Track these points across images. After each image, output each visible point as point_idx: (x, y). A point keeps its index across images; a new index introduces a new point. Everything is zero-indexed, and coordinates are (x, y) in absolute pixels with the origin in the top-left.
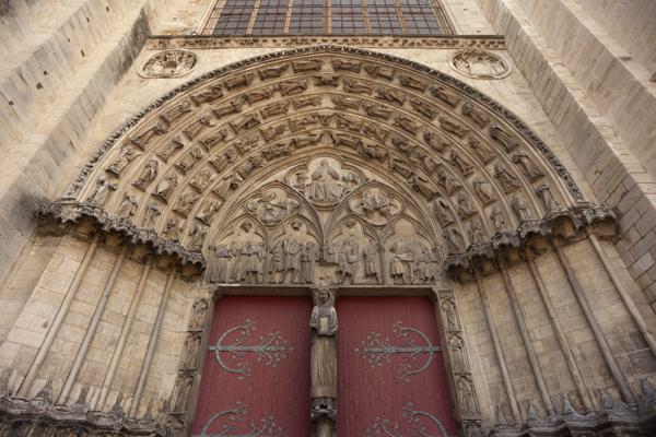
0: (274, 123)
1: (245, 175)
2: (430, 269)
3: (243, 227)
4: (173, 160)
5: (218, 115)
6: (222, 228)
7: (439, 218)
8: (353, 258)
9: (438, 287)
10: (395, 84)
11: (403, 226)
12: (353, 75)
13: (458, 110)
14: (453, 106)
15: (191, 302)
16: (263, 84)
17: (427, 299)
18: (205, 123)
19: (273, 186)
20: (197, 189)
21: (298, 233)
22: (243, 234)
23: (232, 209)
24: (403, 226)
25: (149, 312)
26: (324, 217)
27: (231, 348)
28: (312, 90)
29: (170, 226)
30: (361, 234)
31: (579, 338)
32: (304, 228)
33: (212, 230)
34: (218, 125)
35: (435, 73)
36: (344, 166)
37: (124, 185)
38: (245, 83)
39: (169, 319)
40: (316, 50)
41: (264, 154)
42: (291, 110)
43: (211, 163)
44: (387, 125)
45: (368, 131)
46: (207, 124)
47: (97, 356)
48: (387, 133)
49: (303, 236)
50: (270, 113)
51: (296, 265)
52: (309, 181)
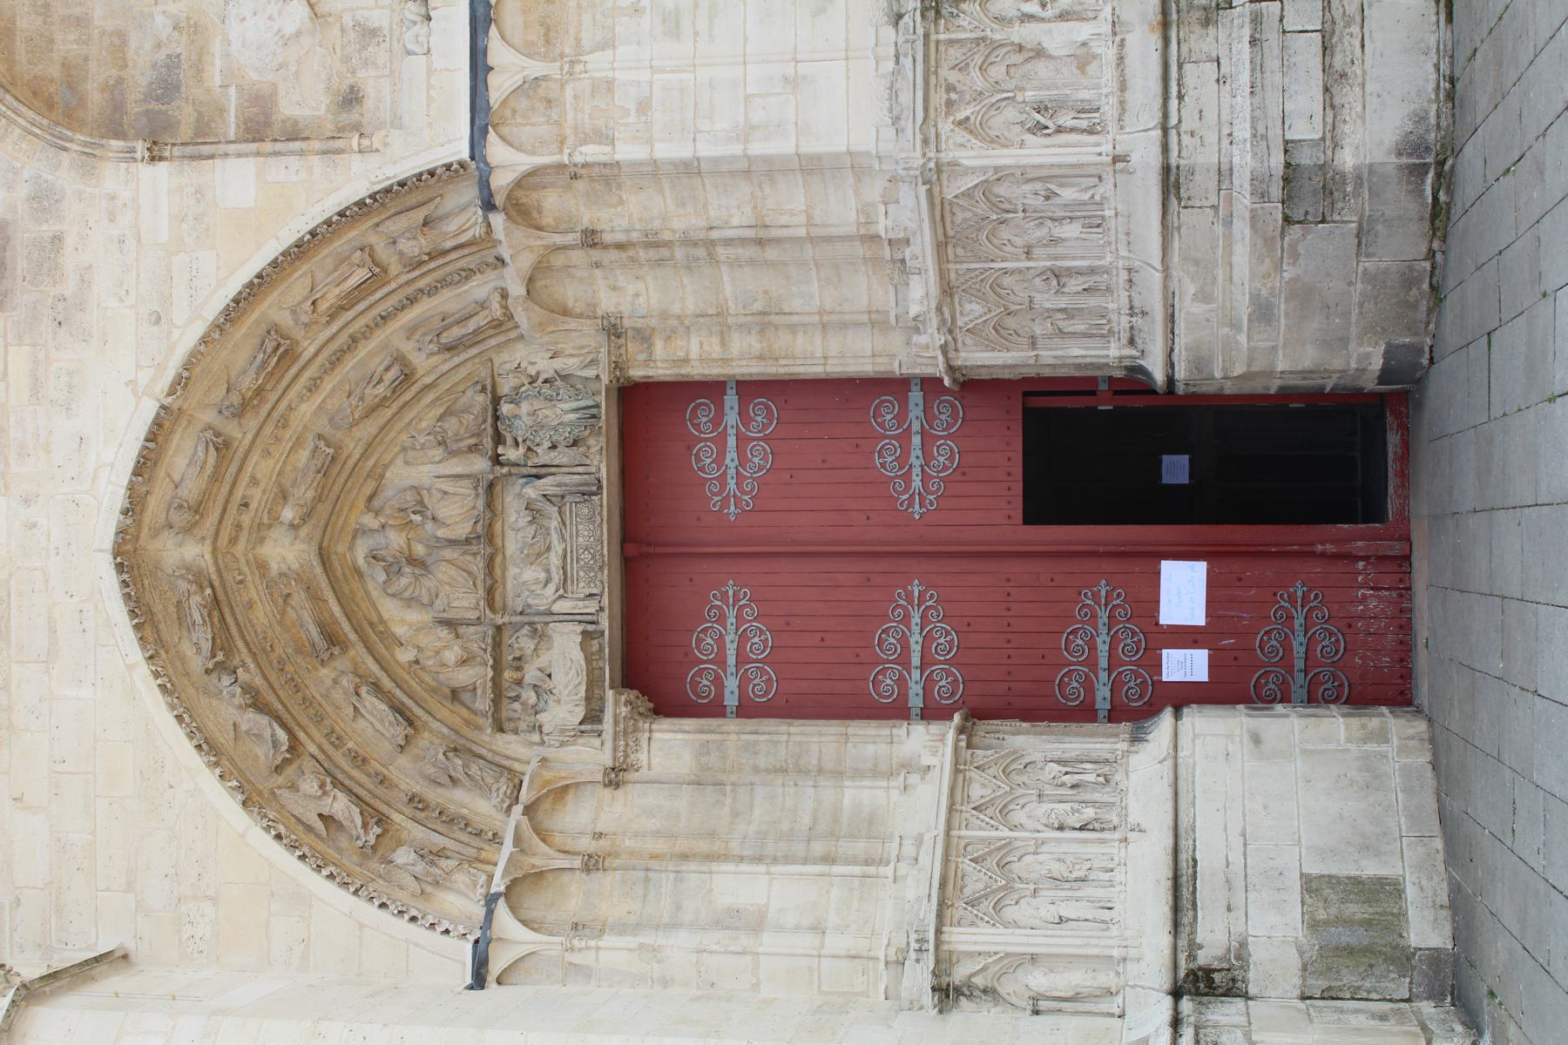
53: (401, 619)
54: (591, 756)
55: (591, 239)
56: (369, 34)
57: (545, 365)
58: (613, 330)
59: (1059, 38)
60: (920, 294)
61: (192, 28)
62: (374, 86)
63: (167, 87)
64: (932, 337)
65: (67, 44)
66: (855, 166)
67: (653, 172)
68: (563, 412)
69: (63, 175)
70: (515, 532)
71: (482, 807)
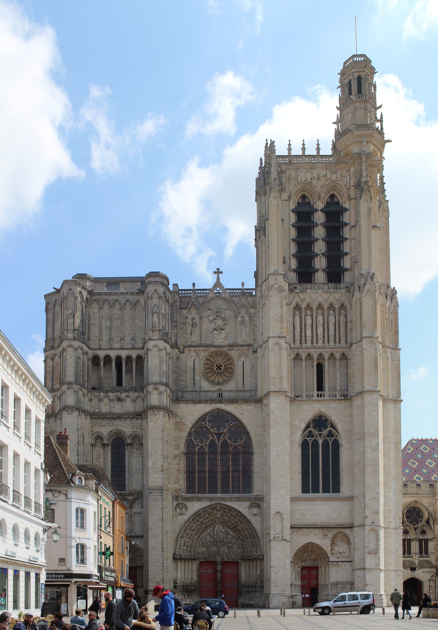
0: (206, 521)
1: (201, 534)
2: (238, 557)
3: (202, 547)
4: (188, 537)
5: (194, 523)
6: (198, 547)
7: (242, 547)
8: (225, 554)
9: (239, 561)
10: (234, 514)
11: (235, 546)
12: (225, 510)
13: (247, 524)
14: (246, 524)
15: (196, 564)
16: (204, 514)
17: (237, 563)
18: (192, 527)
19: (206, 536)
20: (193, 541)
21: (213, 548)
22: (203, 548)
23: (199, 542)
24: (235, 546)
25: (190, 568)
26: (219, 544)
27: (203, 571)
28: (215, 512)
29: (190, 552)
30: (226, 548)
31: (255, 574)
32: (215, 547)
33: (196, 549)
34: (195, 525)
35: (243, 515)
36: (223, 528)
37: (182, 547)
38: (200, 515)
39: (193, 568)
40: (216, 504)
41: (205, 528)
42: (210, 517)
43: (194, 534)
44: (233, 522)
45: (228, 522)
46: (193, 526)
47: (187, 576)
48: (233, 524)
49: (214, 549)
50: (205, 519)
51: (214, 556)
52: (215, 533)
53: (306, 555)
54: (299, 565)
55: (326, 567)
56: (337, 555)
57: (319, 563)
58: (321, 567)
59: (335, 590)
60: (323, 583)
61: (337, 545)
62: (334, 555)
63: (335, 544)
64: (321, 583)
65: (337, 538)
66: (329, 580)
67: (329, 570)
68: (317, 564)
69: (330, 539)
70: (311, 561)
71: (297, 560)
